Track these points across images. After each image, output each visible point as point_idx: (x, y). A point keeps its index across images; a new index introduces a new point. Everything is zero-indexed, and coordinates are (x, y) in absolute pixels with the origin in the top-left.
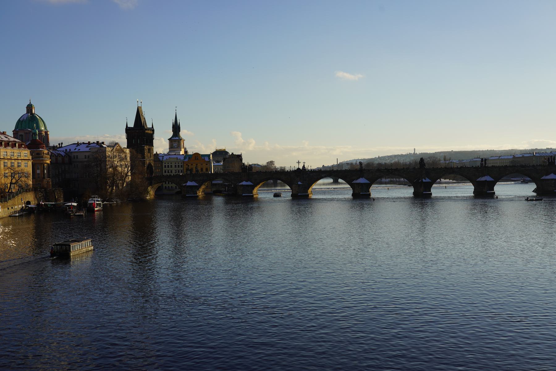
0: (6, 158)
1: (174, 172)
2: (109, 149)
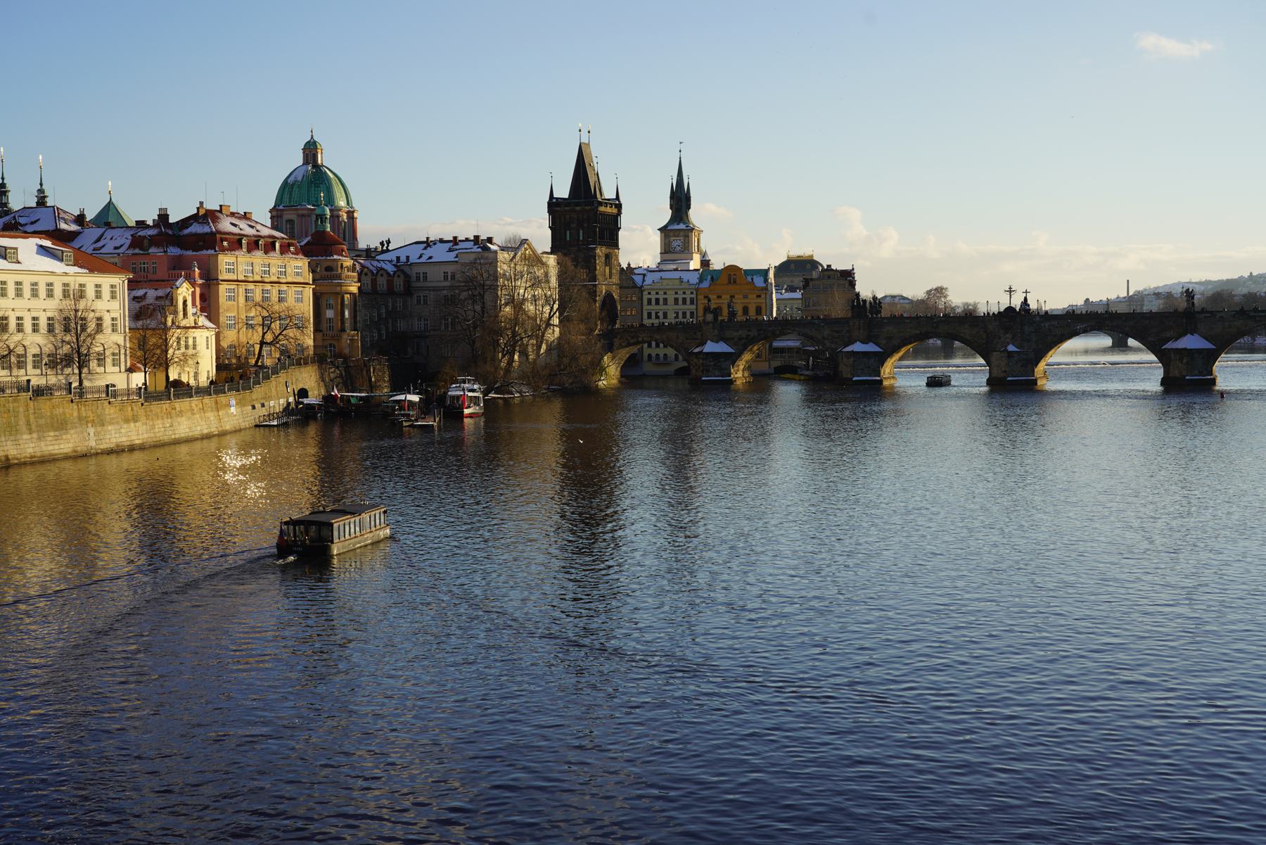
0: (251, 280)
1: (671, 316)
2: (503, 256)
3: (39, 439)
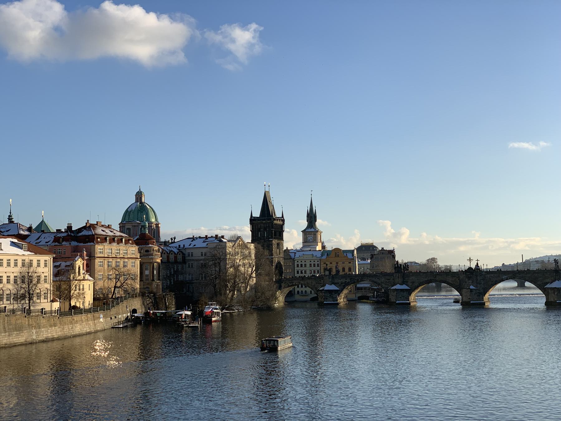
0: (111, 256)
1: (308, 272)
2: (229, 245)
3: (9, 335)
